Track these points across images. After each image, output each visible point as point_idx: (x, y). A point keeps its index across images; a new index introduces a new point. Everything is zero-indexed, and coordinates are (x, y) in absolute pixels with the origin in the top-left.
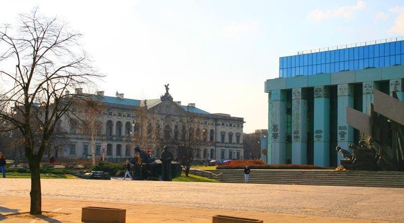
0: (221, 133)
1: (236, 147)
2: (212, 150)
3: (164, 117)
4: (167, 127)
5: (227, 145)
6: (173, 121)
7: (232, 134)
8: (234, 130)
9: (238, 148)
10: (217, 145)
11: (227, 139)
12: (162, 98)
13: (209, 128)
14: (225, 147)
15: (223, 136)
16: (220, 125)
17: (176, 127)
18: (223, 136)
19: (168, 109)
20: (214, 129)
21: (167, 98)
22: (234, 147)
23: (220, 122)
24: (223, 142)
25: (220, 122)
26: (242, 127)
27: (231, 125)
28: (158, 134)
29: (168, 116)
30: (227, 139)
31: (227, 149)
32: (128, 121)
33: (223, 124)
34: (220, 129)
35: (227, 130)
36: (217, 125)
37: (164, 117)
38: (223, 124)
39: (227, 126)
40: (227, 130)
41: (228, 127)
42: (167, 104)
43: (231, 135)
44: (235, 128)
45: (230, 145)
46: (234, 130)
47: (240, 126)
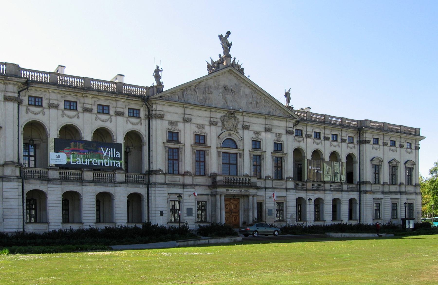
0: (372, 160)
1: (406, 193)
2: (351, 202)
3: (218, 115)
4: (230, 143)
5: (386, 189)
6: (246, 128)
7: (398, 162)
8: (401, 155)
9: (411, 193)
10: (363, 188)
11: (385, 176)
12: (214, 67)
13: (344, 151)
14: (384, 193)
15: (377, 168)
16: (368, 142)
17: (257, 144)
18: (377, 168)
19: (229, 97)
20: (355, 152)
21: (225, 68)
22: (401, 193)
23: (368, 136)
24: (377, 181)
25: (368, 136)
26: (418, 148)
27: (393, 144)
28: (201, 158)
29: (231, 114)
30: (385, 176)
31: (388, 198)
32: (66, 121)
33: (376, 141)
34: (370, 151)
35: (386, 154)
36: (360, 142)
37: (218, 115)
38: (376, 141)
39: (385, 144)
40: (386, 154)
41: (387, 148)
42: (227, 83)
43: (394, 167)
44: (403, 150)
45: (393, 188)
46: (401, 155)
47: (413, 147)
